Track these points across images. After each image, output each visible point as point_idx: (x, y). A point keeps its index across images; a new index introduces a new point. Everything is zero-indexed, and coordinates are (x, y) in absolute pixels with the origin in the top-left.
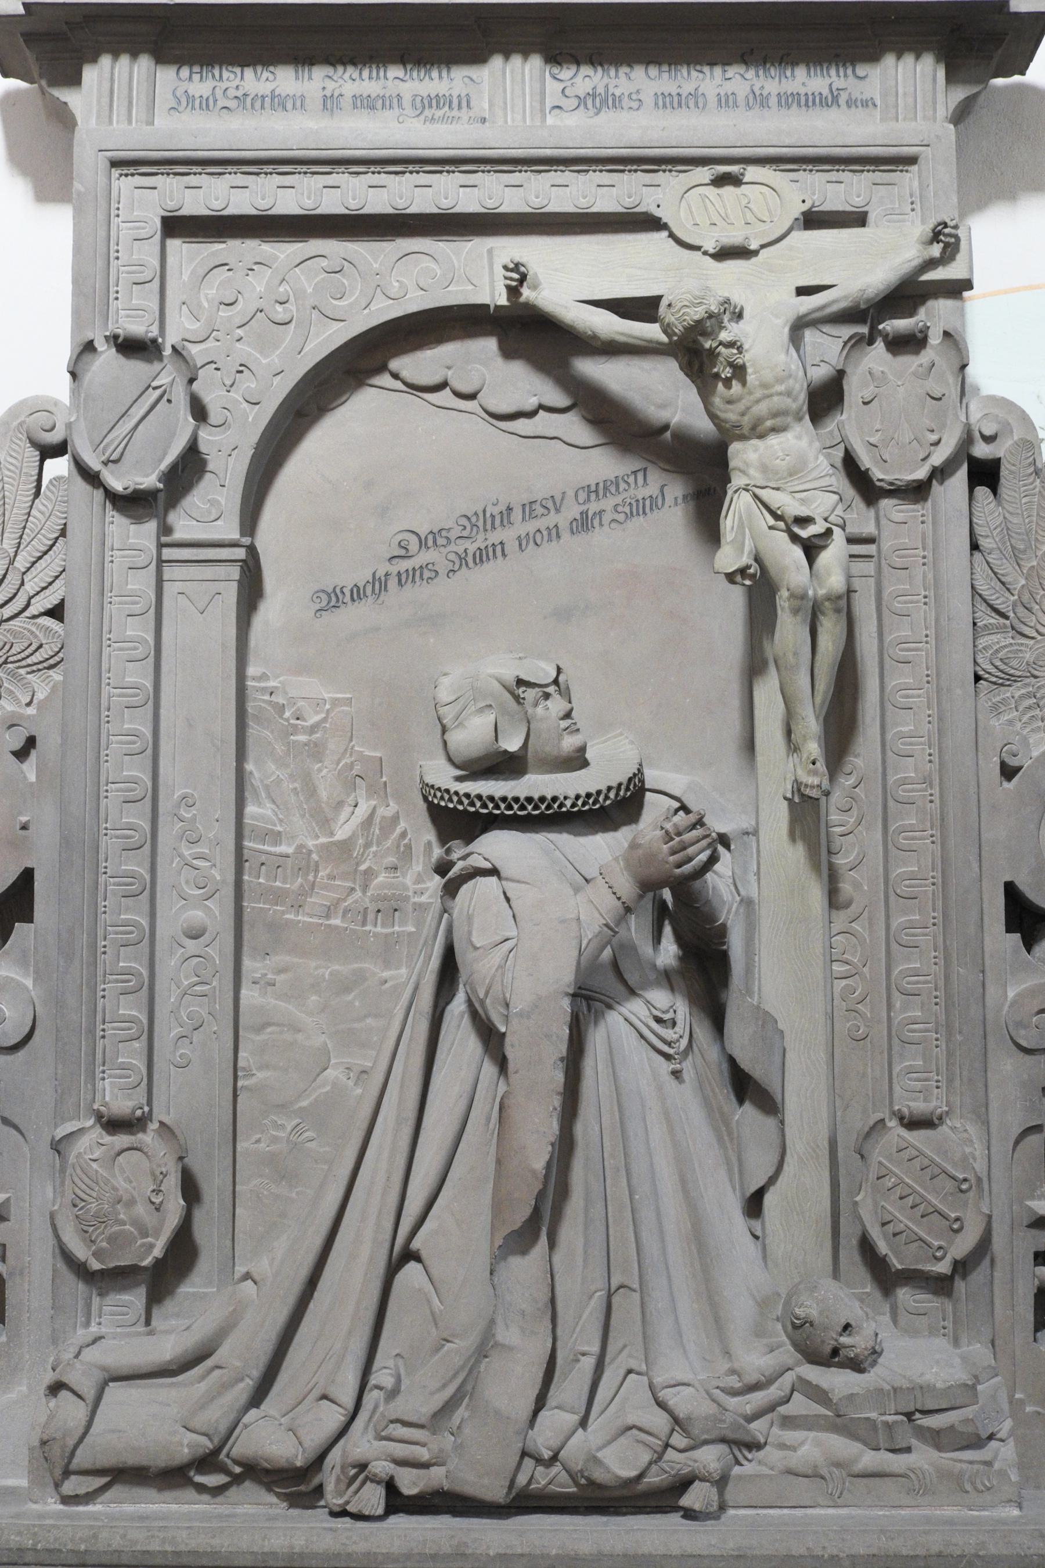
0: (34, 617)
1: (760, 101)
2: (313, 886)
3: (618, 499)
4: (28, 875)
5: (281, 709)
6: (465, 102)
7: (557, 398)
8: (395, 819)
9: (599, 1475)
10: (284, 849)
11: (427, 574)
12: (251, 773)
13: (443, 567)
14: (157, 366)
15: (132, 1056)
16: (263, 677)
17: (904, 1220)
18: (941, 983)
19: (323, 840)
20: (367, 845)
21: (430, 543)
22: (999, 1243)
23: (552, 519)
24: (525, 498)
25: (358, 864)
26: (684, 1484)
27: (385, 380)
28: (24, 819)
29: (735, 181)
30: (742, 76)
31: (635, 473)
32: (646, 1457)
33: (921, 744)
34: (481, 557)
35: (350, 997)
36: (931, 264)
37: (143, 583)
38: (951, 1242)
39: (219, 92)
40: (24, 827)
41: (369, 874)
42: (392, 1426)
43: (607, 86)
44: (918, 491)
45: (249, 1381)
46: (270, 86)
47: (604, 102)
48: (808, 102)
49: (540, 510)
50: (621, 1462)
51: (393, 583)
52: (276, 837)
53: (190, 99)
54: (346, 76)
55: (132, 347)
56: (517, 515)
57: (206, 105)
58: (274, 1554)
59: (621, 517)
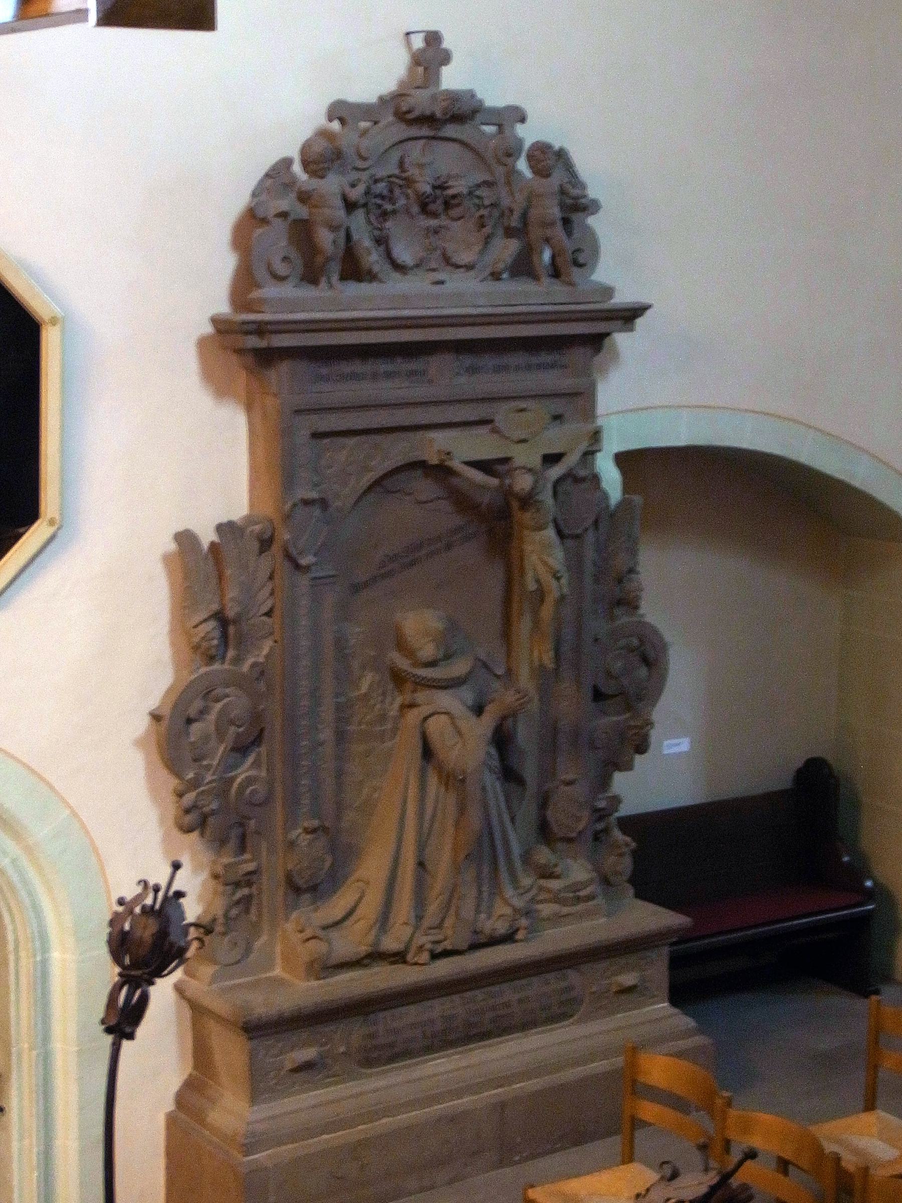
34: (412, 564)
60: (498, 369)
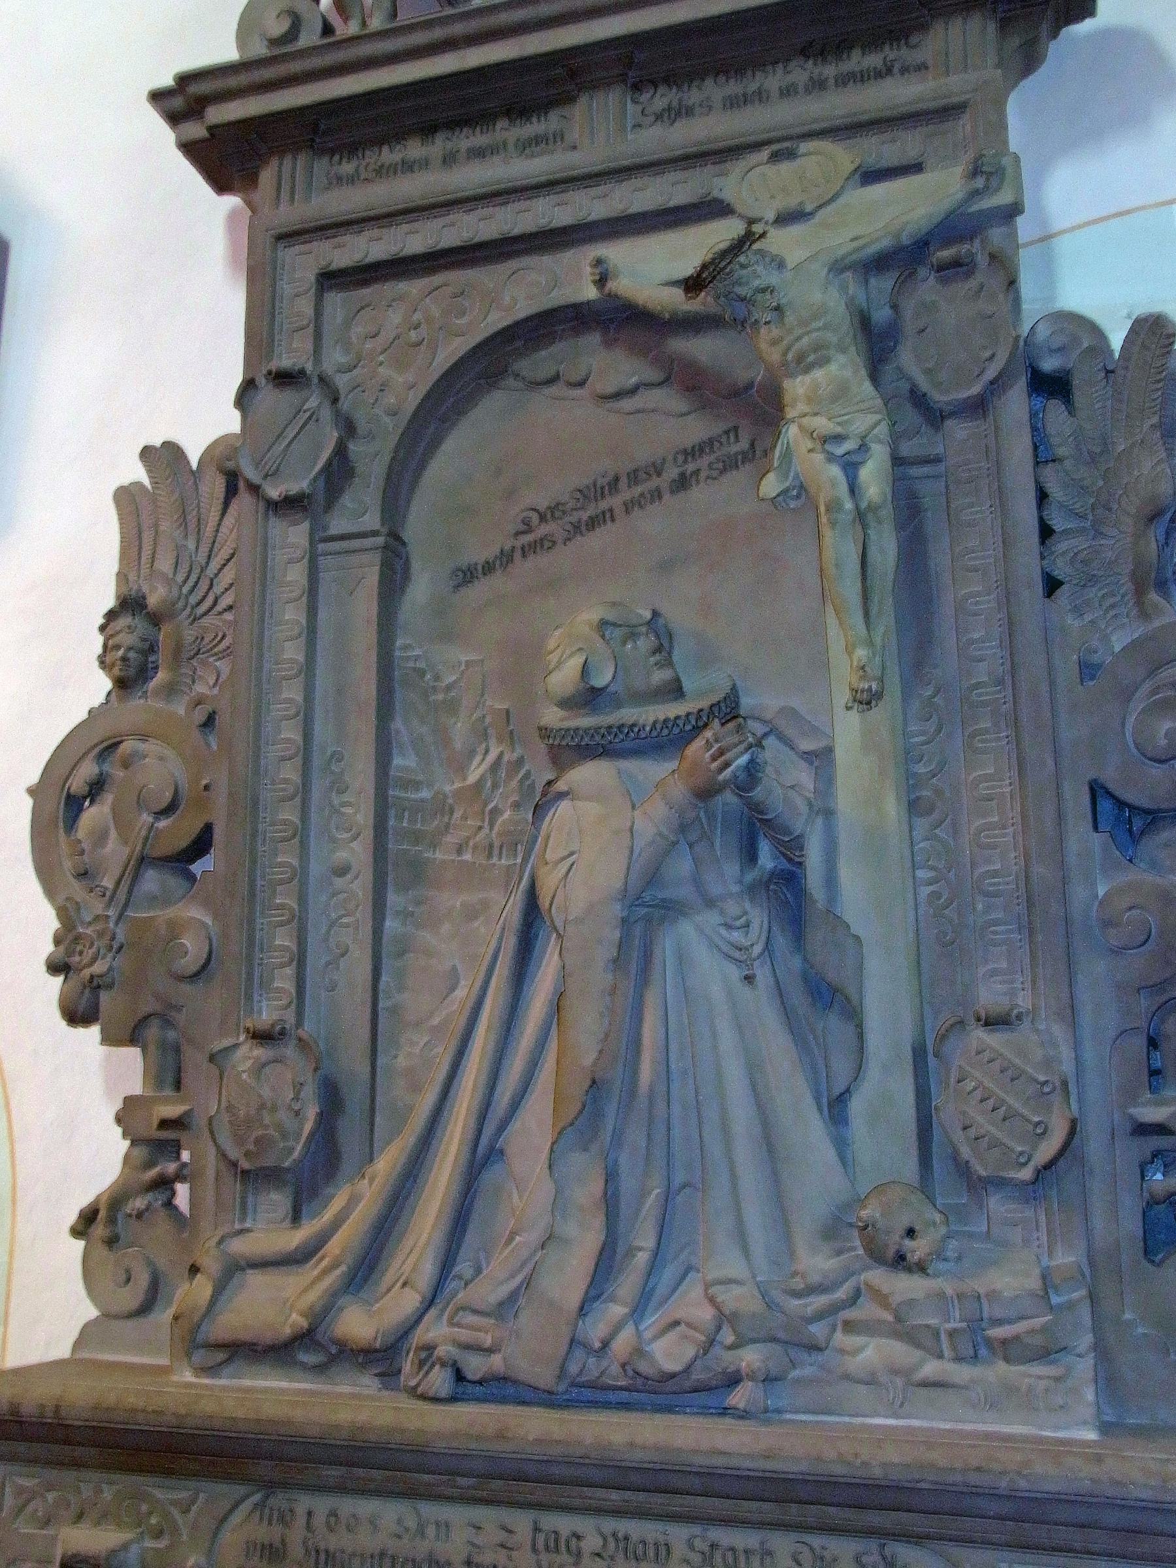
0: (220, 613)
1: (818, 85)
2: (447, 826)
3: (712, 458)
4: (208, 829)
5: (421, 673)
6: (559, 136)
7: (652, 374)
8: (520, 762)
9: (643, 1367)
10: (425, 794)
11: (547, 544)
12: (398, 732)
13: (560, 535)
14: (305, 393)
15: (284, 981)
16: (406, 647)
17: (983, 1123)
18: (1022, 885)
19: (457, 785)
20: (495, 786)
21: (549, 516)
22: (1094, 1146)
23: (655, 482)
24: (630, 467)
25: (486, 805)
26: (733, 1380)
27: (511, 382)
28: (204, 782)
29: (791, 155)
30: (802, 67)
31: (727, 432)
32: (690, 1352)
33: (992, 648)
34: (593, 523)
35: (476, 925)
36: (975, 194)
37: (297, 575)
38: (1035, 1147)
39: (362, 169)
40: (206, 788)
41: (495, 812)
42: (461, 1313)
43: (680, 100)
44: (979, 407)
45: (344, 1268)
46: (401, 156)
47: (678, 114)
48: (862, 77)
49: (643, 476)
50: (669, 1354)
51: (518, 555)
52: (417, 785)
53: (339, 179)
54: (462, 136)
55: (285, 378)
56: (623, 482)
57: (352, 180)
58: (337, 1427)
59: (715, 473)
60: (733, 103)
